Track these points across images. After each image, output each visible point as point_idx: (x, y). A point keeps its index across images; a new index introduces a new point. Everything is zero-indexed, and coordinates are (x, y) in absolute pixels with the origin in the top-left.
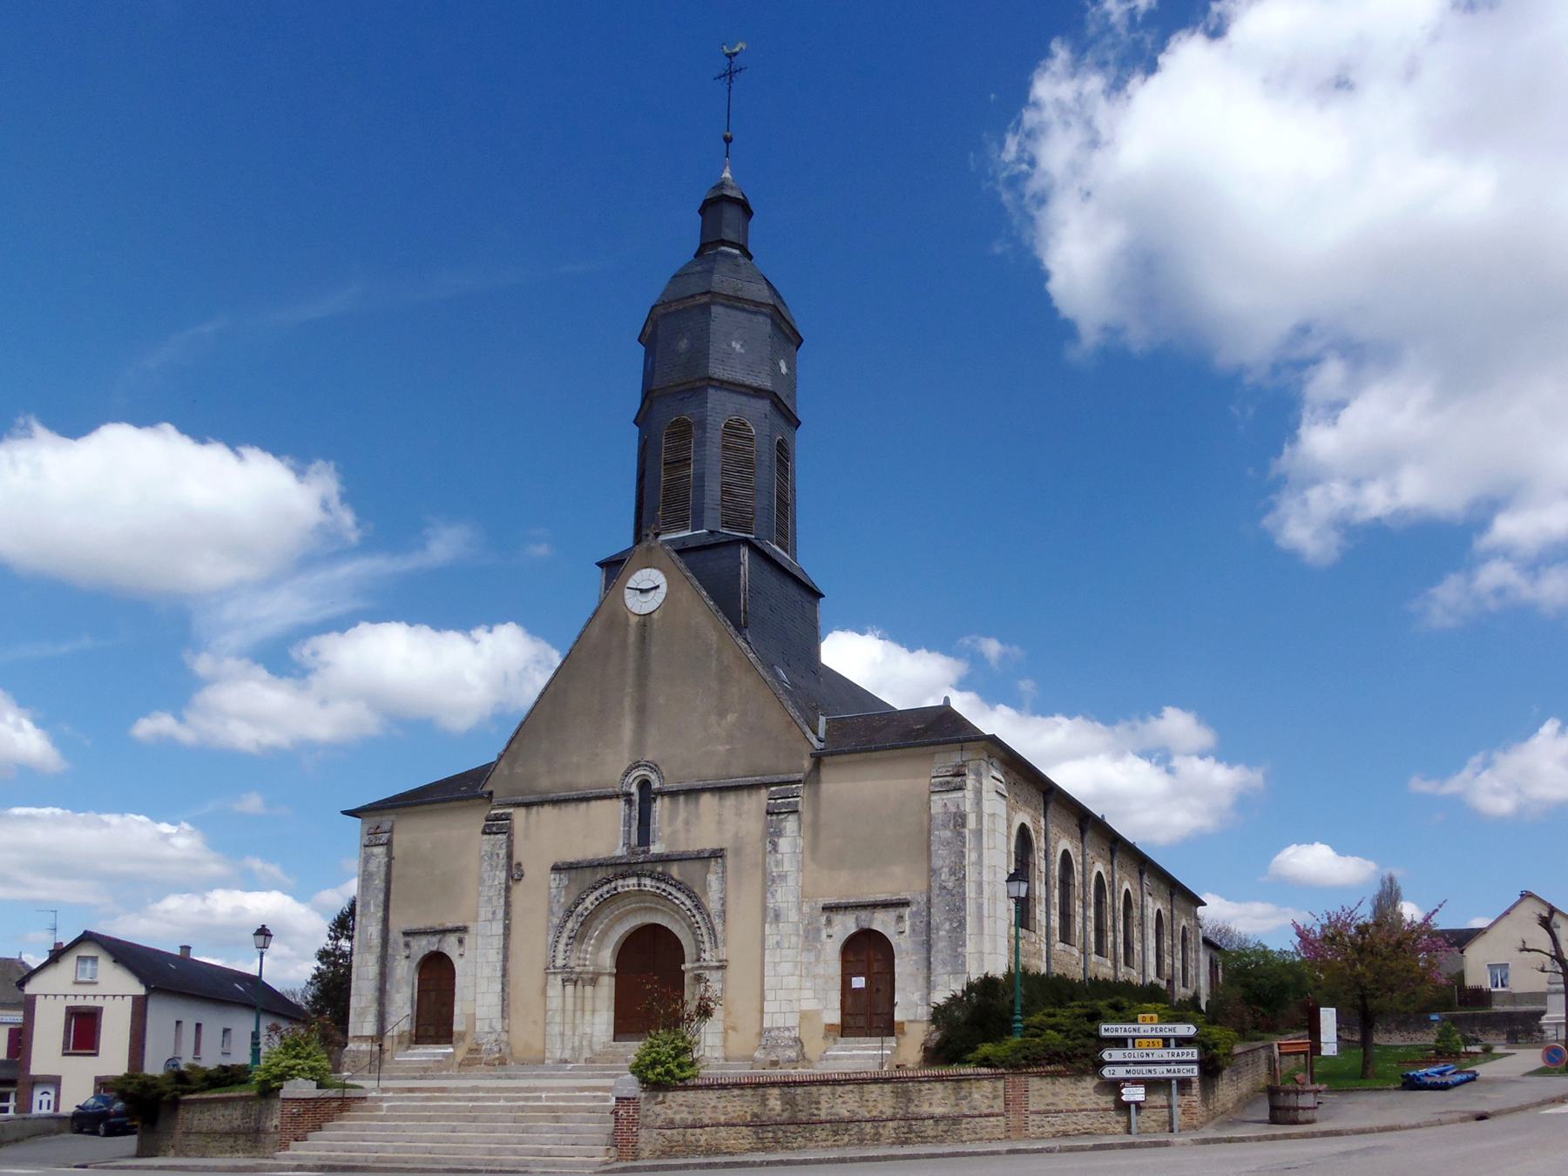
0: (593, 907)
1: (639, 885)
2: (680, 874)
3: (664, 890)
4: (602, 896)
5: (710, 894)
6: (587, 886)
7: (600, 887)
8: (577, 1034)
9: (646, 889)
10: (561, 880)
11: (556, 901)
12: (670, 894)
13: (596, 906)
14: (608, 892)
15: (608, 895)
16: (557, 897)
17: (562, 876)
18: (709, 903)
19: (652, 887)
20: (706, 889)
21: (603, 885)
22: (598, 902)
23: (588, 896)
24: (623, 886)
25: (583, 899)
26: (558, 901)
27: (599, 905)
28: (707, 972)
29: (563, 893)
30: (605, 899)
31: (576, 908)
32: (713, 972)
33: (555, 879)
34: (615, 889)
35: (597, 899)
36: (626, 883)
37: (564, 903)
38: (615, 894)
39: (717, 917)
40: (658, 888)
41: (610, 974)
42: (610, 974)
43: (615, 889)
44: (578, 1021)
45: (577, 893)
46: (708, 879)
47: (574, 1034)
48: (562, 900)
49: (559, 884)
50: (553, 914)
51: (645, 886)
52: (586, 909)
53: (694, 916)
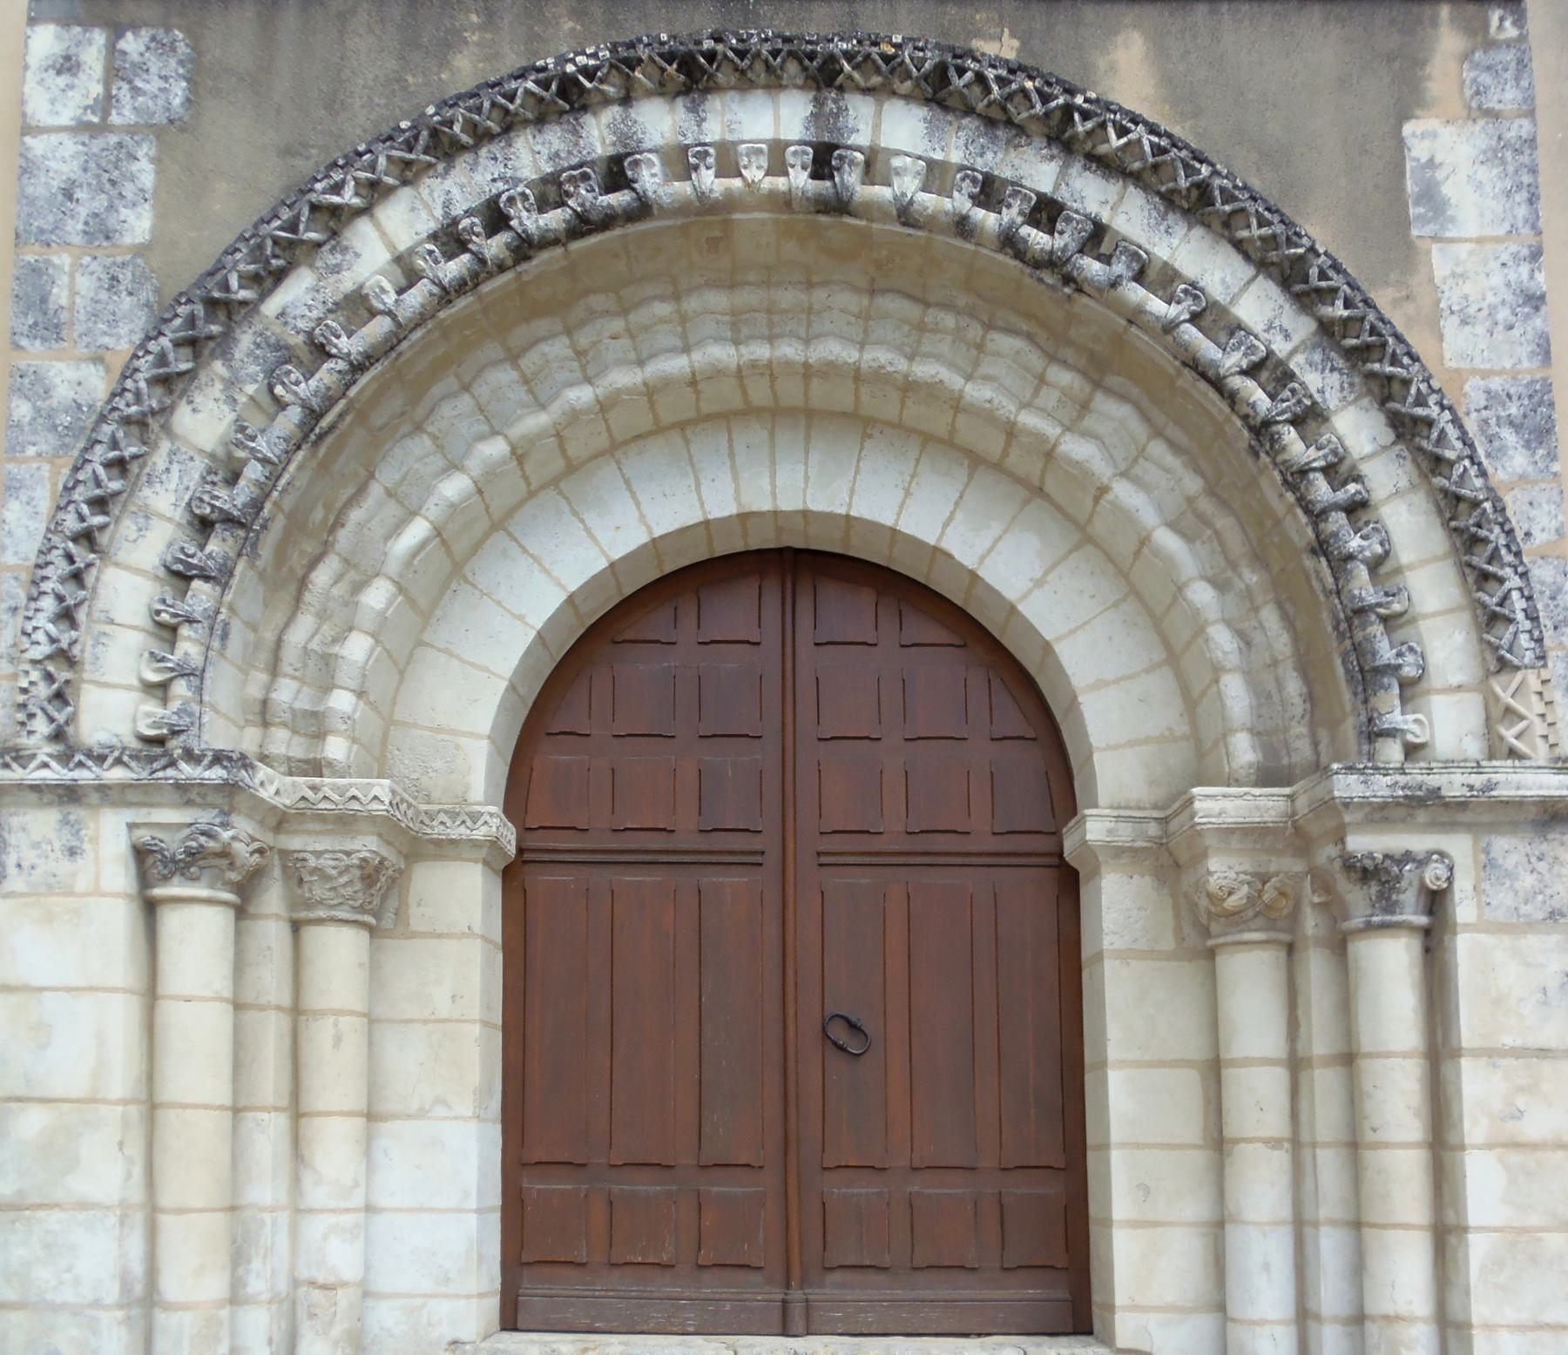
0: (416, 297)
1: (824, 160)
2: (1173, 87)
3: (1047, 212)
4: (495, 217)
5: (1440, 262)
6: (357, 126)
7: (482, 137)
8: (257, 1285)
9: (882, 193)
10: (116, 70)
11: (74, 227)
12: (1096, 236)
13: (447, 294)
14: (550, 192)
15: (555, 219)
16: (88, 203)
17: (131, 44)
18: (1433, 322)
19: (936, 175)
20: (1404, 223)
21: (510, 125)
22: (454, 269)
23: (375, 192)
24: (681, 161)
25: (335, 219)
26: (101, 232)
27: (461, 287)
28: (1459, 846)
29: (145, 172)
30: (525, 248)
31: (269, 279)
32: (1510, 848)
33: (67, 65)
34: (616, 173)
35: (451, 239)
36: (713, 131)
37: (141, 250)
38: (609, 220)
39: (1508, 435)
40: (989, 192)
41: (1424, 1320)
42: (1424, 1320)
43: (616, 173)
44: (265, 1190)
45: (272, 179)
46: (1418, 150)
47: (236, 1297)
48: (138, 224)
49: (107, 102)
50: (49, 327)
51: (875, 165)
52: (357, 306)
53: (1309, 417)
